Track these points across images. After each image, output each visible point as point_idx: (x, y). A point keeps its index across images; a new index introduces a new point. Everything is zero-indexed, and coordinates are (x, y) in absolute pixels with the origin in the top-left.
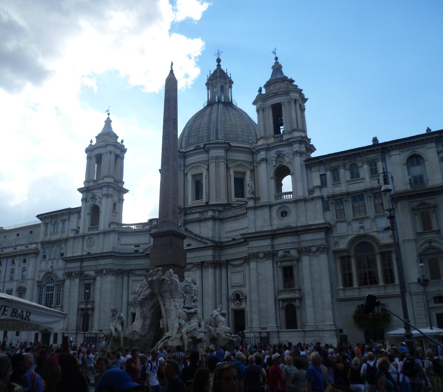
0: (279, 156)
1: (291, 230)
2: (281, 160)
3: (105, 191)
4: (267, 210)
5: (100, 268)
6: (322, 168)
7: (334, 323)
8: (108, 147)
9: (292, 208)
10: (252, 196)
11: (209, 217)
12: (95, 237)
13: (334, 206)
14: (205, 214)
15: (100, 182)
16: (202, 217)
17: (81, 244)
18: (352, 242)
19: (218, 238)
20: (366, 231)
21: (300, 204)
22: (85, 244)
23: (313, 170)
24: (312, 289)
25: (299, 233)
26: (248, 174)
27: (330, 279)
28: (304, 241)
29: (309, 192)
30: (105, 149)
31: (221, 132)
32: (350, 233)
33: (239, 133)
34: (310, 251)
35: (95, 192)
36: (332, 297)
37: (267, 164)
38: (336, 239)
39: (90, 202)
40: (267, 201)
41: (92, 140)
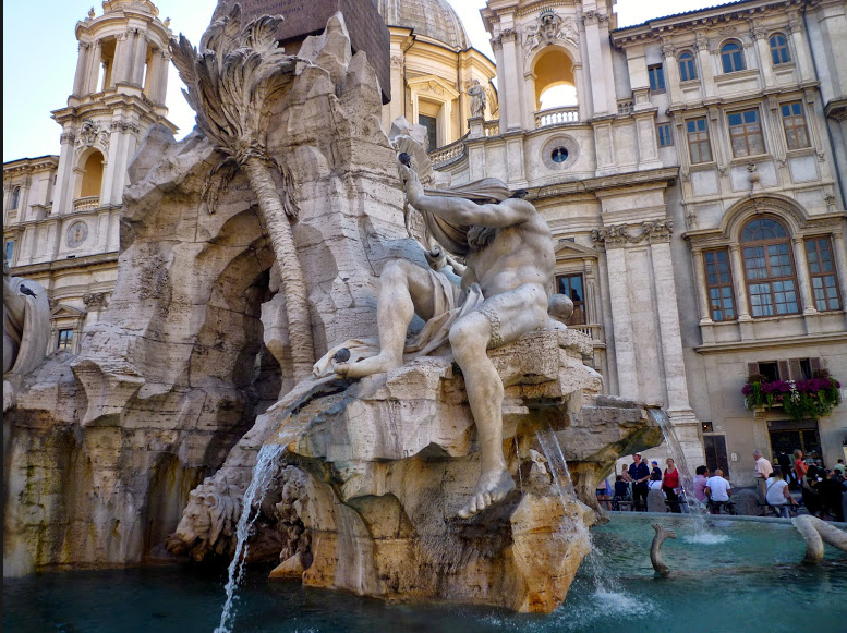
0: (548, 22)
1: (581, 188)
2: (553, 34)
3: (118, 115)
4: (515, 147)
5: (97, 291)
6: (653, 49)
7: (690, 404)
8: (131, 20)
9: (581, 138)
10: (480, 115)
12: (89, 222)
13: (686, 132)
15: (107, 95)
17: (52, 237)
18: (734, 214)
20: (768, 190)
21: (600, 130)
22: (63, 238)
23: (629, 55)
24: (633, 325)
25: (599, 195)
26: (448, 107)
27: (678, 300)
28: (611, 214)
29: (620, 105)
30: (124, 27)
31: (393, 13)
32: (726, 194)
33: (429, 21)
34: (628, 238)
35: (95, 119)
36: (684, 342)
37: (516, 45)
38: (690, 209)
39: (82, 143)
40: (517, 125)
41: (92, 10)
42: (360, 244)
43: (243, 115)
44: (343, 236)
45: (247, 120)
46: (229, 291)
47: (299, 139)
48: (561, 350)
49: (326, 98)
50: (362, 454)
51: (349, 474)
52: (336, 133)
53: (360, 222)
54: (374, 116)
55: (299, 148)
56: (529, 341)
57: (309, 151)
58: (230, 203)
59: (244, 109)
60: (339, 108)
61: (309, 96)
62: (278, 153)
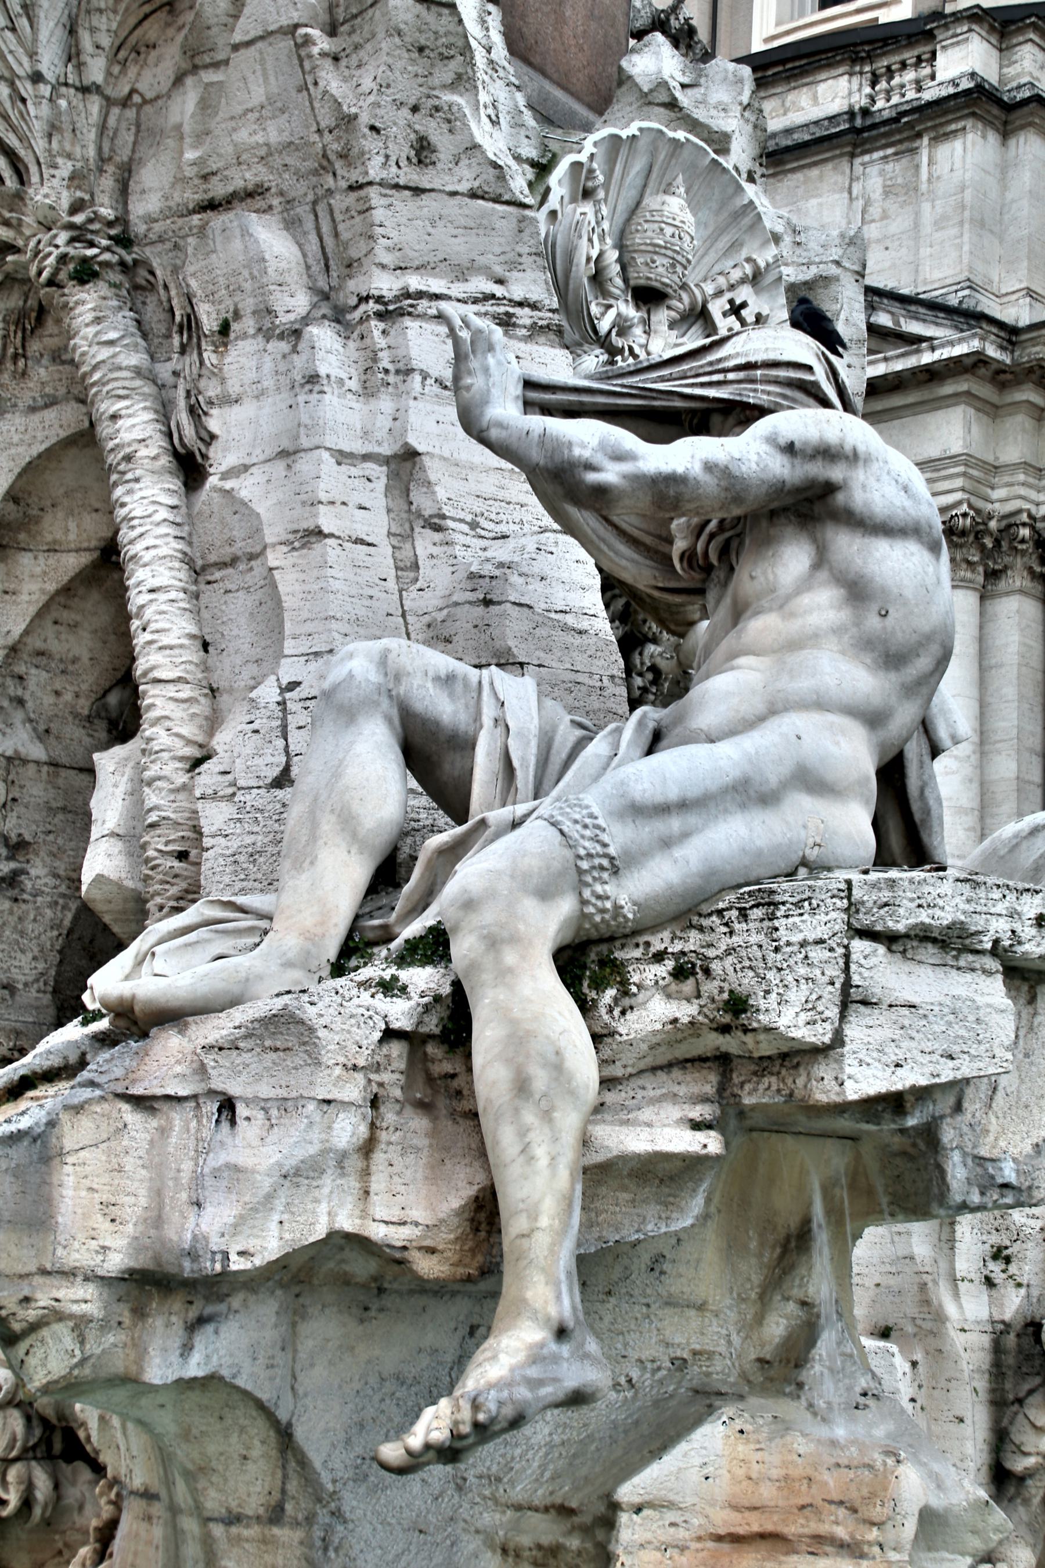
11: (951, 90)
14: (910, 75)
16: (880, 104)
19: (1030, 293)
42: (383, 559)
43: (38, 113)
44: (319, 533)
45: (52, 130)
46: (49, 700)
47: (219, 189)
48: (859, 946)
49: (286, 44)
50: (80, 1256)
51: (32, 1314)
52: (325, 165)
53: (393, 476)
54: (448, 97)
55: (218, 221)
56: (734, 913)
57: (245, 233)
58: (33, 409)
59: (45, 90)
60: (331, 80)
61: (238, 37)
62: (161, 240)
